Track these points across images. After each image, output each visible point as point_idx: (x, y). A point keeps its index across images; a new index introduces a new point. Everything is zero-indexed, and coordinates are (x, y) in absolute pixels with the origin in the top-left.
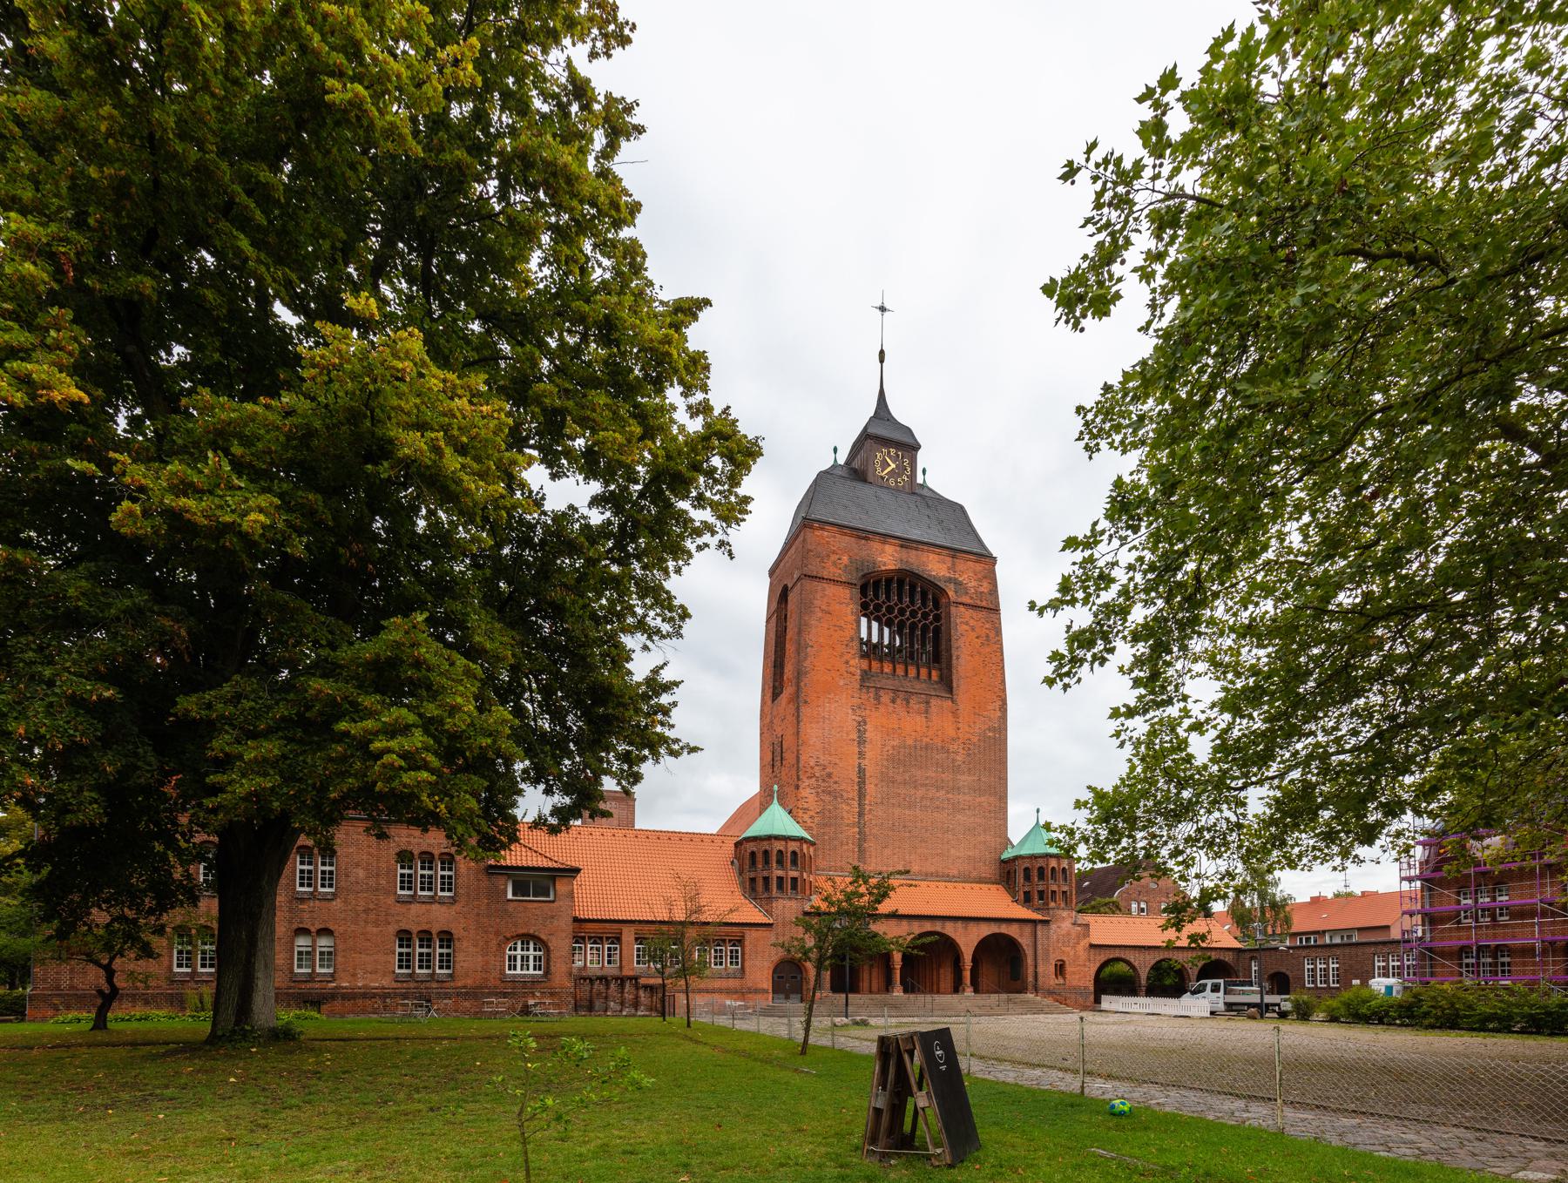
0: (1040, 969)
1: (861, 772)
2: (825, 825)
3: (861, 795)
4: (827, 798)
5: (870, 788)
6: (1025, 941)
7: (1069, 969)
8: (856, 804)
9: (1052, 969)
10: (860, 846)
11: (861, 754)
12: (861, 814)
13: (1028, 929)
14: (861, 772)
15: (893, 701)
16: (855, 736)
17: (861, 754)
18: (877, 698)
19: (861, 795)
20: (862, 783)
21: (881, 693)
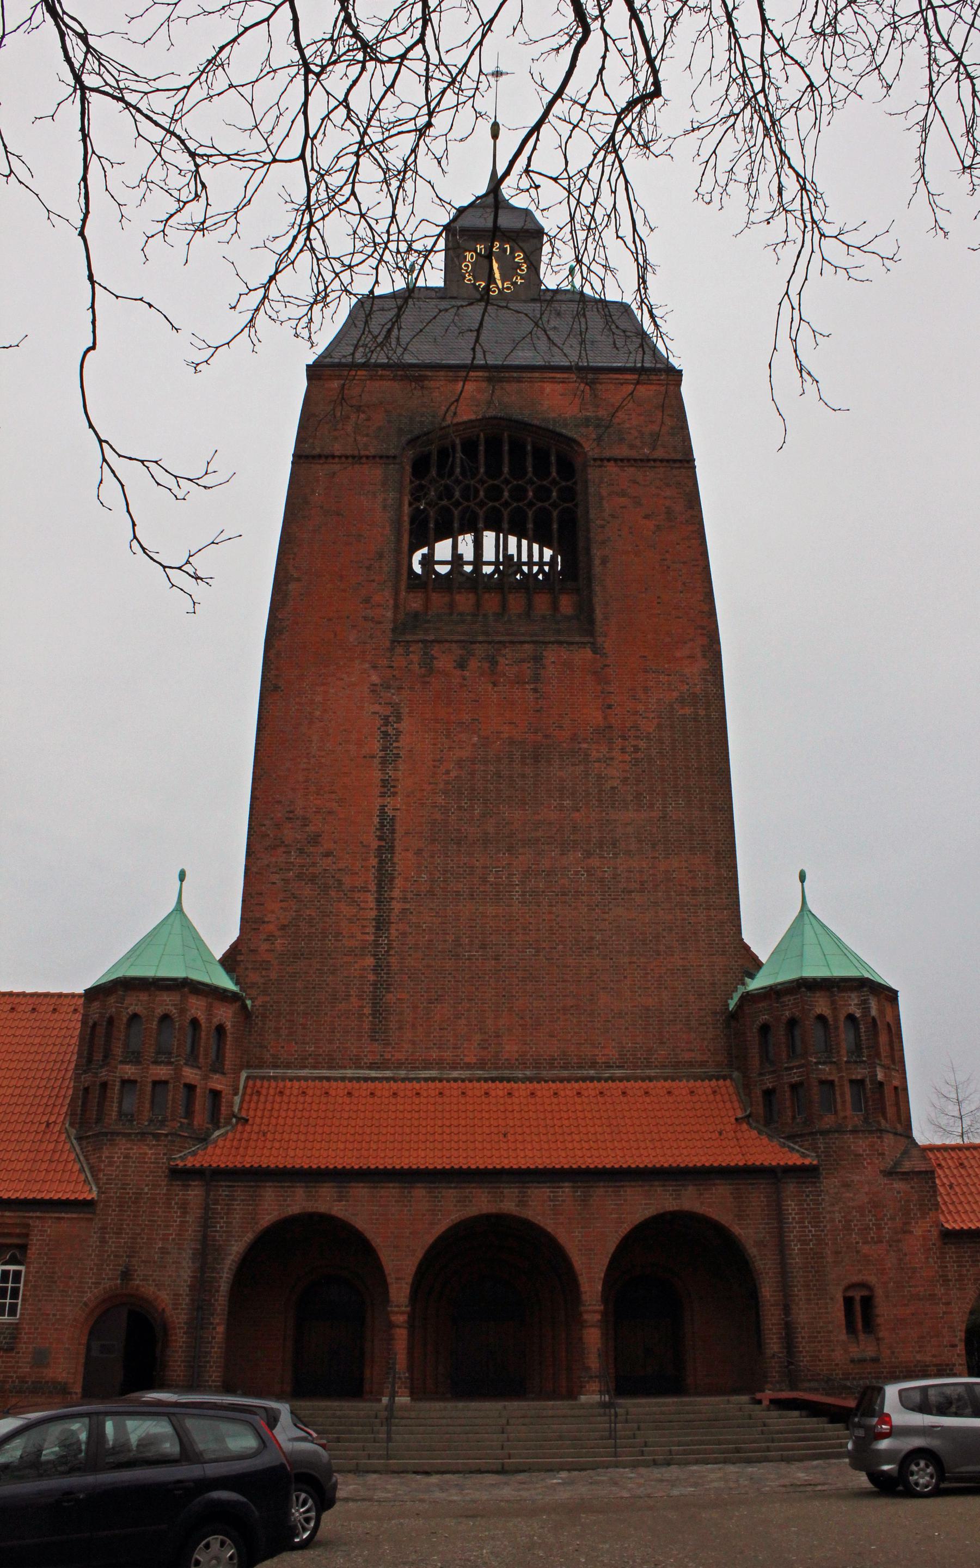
0: (801, 1316)
1: (386, 825)
3: (384, 879)
5: (403, 860)
6: (750, 1232)
7: (884, 1311)
8: (371, 898)
9: (838, 1313)
11: (387, 786)
12: (381, 924)
13: (757, 1197)
14: (386, 825)
15: (462, 665)
16: (377, 746)
17: (387, 786)
19: (384, 879)
20: (386, 848)
21: (435, 650)
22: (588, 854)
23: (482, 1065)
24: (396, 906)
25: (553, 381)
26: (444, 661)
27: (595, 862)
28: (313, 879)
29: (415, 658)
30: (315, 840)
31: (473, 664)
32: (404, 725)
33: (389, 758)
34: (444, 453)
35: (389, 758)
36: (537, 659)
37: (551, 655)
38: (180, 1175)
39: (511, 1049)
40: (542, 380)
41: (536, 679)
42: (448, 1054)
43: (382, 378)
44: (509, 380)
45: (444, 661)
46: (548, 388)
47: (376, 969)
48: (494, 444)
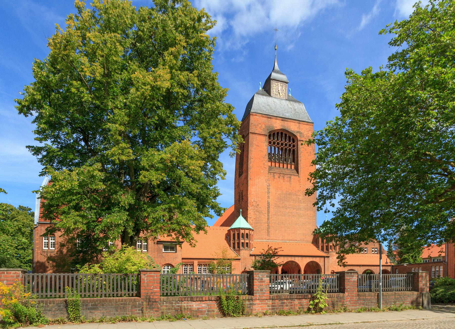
1: (268, 203)
2: (257, 223)
3: (268, 212)
4: (257, 213)
5: (271, 209)
8: (267, 215)
10: (268, 230)
12: (268, 219)
14: (268, 203)
15: (279, 178)
18: (274, 176)
19: (268, 212)
20: (269, 207)
21: (275, 174)
22: (297, 210)
23: (282, 240)
24: (270, 216)
25: (293, 122)
26: (276, 176)
27: (298, 211)
28: (258, 211)
29: (272, 175)
30: (258, 205)
31: (281, 177)
32: (270, 187)
33: (268, 193)
34: (274, 134)
35: (268, 193)
36: (290, 178)
37: (292, 177)
38: (251, 255)
39: (286, 238)
40: (291, 122)
41: (290, 181)
42: (278, 238)
43: (263, 117)
44: (285, 121)
45: (276, 176)
46: (292, 123)
47: (268, 226)
48: (282, 133)
